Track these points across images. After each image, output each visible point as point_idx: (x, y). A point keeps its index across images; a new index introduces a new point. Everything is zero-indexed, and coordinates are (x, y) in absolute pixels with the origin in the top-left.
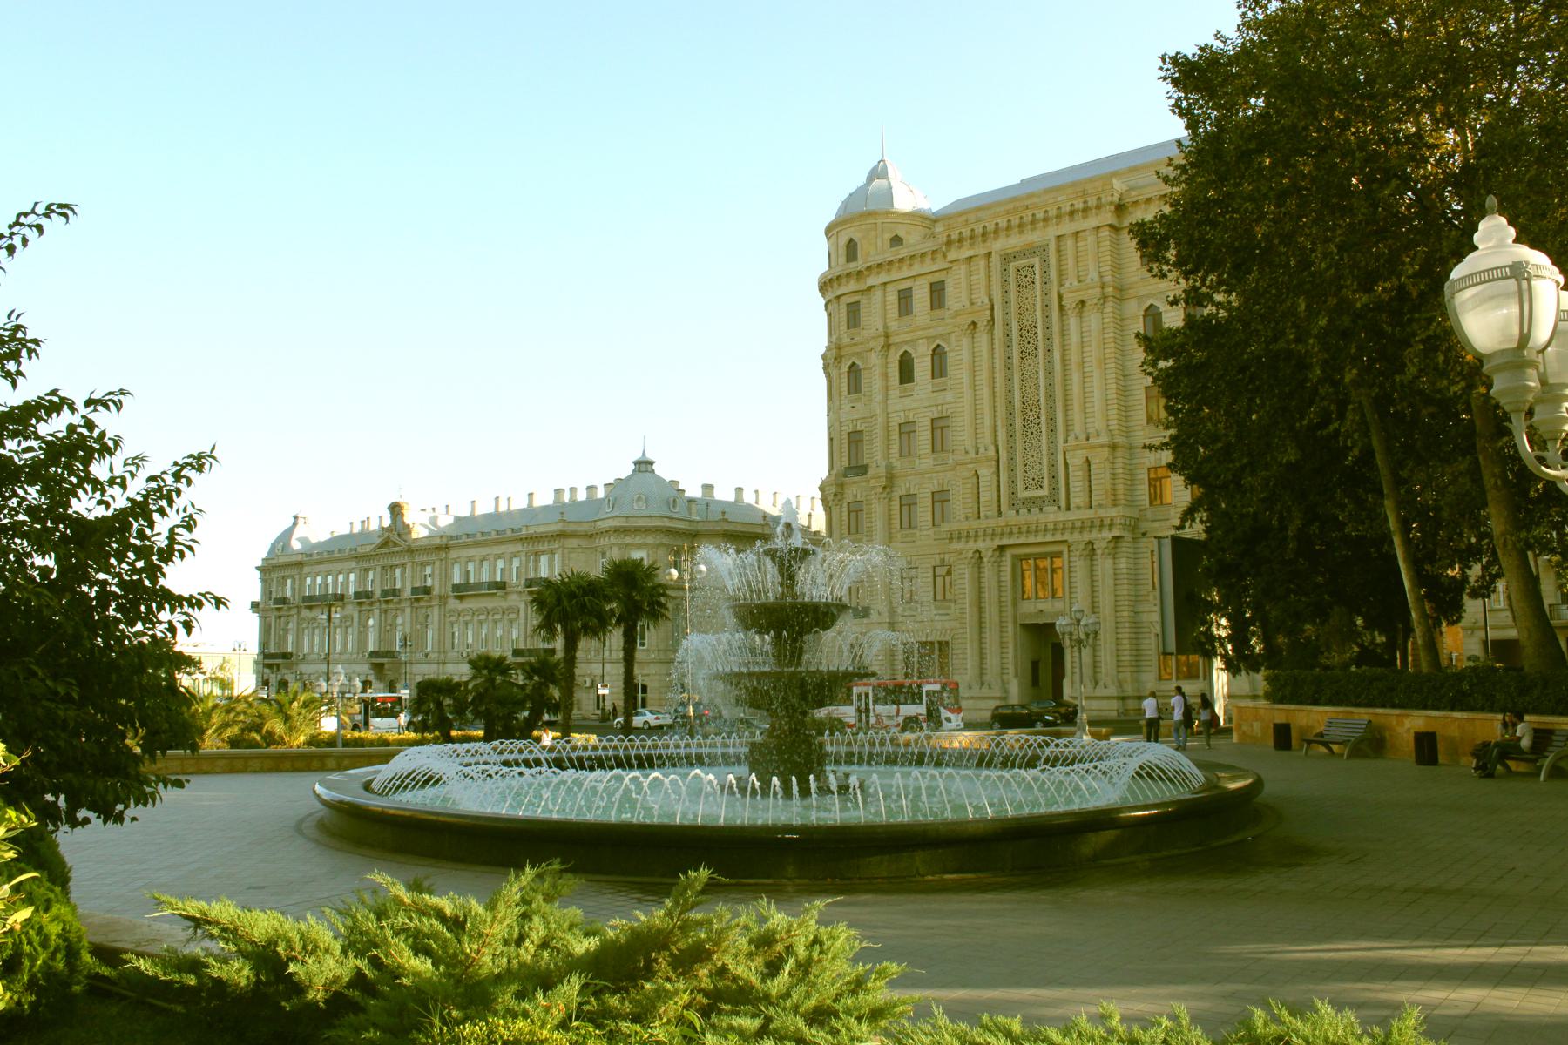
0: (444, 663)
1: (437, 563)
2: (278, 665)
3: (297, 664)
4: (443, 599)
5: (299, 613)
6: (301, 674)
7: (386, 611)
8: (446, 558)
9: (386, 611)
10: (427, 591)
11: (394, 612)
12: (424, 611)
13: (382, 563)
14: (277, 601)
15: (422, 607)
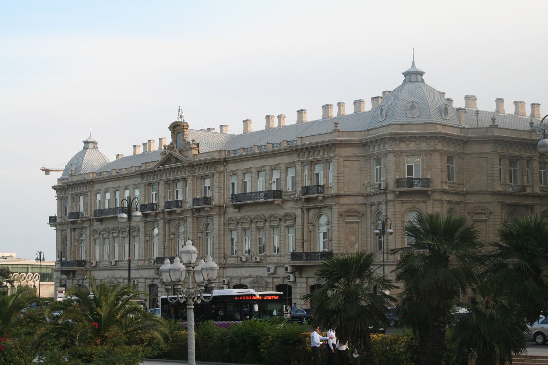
4: (222, 208)
7: (169, 221)
10: (207, 201)
11: (177, 222)
13: (165, 177)
15: (204, 217)
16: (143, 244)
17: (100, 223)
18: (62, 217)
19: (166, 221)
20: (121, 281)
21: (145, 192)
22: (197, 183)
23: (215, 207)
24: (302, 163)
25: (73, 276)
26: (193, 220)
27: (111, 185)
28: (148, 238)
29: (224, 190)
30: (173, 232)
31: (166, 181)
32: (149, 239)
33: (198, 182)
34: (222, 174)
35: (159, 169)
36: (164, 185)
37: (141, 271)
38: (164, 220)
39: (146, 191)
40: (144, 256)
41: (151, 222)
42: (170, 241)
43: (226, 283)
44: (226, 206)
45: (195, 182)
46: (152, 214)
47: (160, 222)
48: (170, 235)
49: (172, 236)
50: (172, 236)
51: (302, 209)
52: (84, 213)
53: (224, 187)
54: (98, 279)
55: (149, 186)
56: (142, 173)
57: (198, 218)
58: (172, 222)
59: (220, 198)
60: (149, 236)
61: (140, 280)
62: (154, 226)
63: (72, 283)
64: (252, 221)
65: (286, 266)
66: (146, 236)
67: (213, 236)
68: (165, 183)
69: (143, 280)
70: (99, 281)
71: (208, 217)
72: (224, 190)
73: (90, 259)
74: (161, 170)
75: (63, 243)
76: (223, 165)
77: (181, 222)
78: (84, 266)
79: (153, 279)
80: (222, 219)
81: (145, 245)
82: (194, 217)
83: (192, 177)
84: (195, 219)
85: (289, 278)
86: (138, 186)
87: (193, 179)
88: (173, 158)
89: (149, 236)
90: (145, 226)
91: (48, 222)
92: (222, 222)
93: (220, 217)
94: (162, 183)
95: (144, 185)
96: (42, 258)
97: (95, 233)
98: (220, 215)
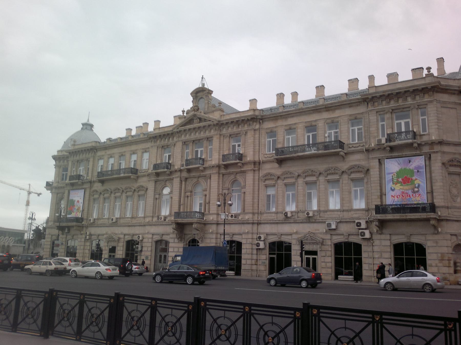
0: (259, 224)
1: (250, 134)
2: (69, 228)
3: (87, 227)
4: (257, 164)
5: (91, 187)
6: (90, 235)
7: (186, 179)
8: (259, 129)
9: (186, 179)
10: (240, 157)
11: (195, 180)
12: (232, 177)
13: (183, 138)
14: (72, 178)
15: (230, 174)
16: (152, 201)
17: (101, 184)
18: (58, 182)
19: (183, 179)
20: (122, 236)
21: (157, 154)
22: (223, 141)
23: (249, 163)
24: (377, 112)
25: (68, 232)
26: (219, 177)
27: (116, 151)
28: (157, 196)
29: (259, 146)
30: (190, 189)
31: (185, 142)
32: (159, 197)
33: (225, 140)
34: (257, 132)
35: (178, 130)
36: (182, 145)
37: (147, 227)
38: (180, 178)
39: (158, 153)
40: (153, 213)
41: (163, 181)
42: (186, 198)
43: (262, 239)
44: (262, 162)
45: (222, 141)
46: (167, 173)
47: (175, 180)
48: (185, 192)
49: (189, 194)
50: (189, 194)
51: (379, 160)
52: (85, 176)
53: (259, 144)
54: (95, 235)
55: (162, 148)
56: (156, 137)
57: (223, 175)
58: (189, 181)
59: (254, 155)
60: (159, 195)
61: (146, 236)
62: (165, 184)
63: (66, 238)
64: (123, 191)
65: (356, 221)
66: (155, 194)
67: (245, 193)
68: (182, 143)
69: (150, 236)
70: (96, 236)
71: (237, 173)
72: (259, 146)
73: (87, 217)
74: (180, 131)
75: (58, 203)
76: (258, 123)
77: (201, 180)
78: (82, 222)
79: (163, 235)
80: (257, 175)
81: (154, 203)
82: (219, 173)
83: (218, 136)
84: (221, 175)
85: (363, 234)
86: (147, 150)
87: (220, 137)
88: (196, 119)
89: (158, 196)
90: (155, 185)
91: (45, 186)
92: (257, 177)
93: (254, 173)
94: (179, 145)
95: (157, 147)
96: (33, 218)
97: (95, 193)
98: (254, 171)
